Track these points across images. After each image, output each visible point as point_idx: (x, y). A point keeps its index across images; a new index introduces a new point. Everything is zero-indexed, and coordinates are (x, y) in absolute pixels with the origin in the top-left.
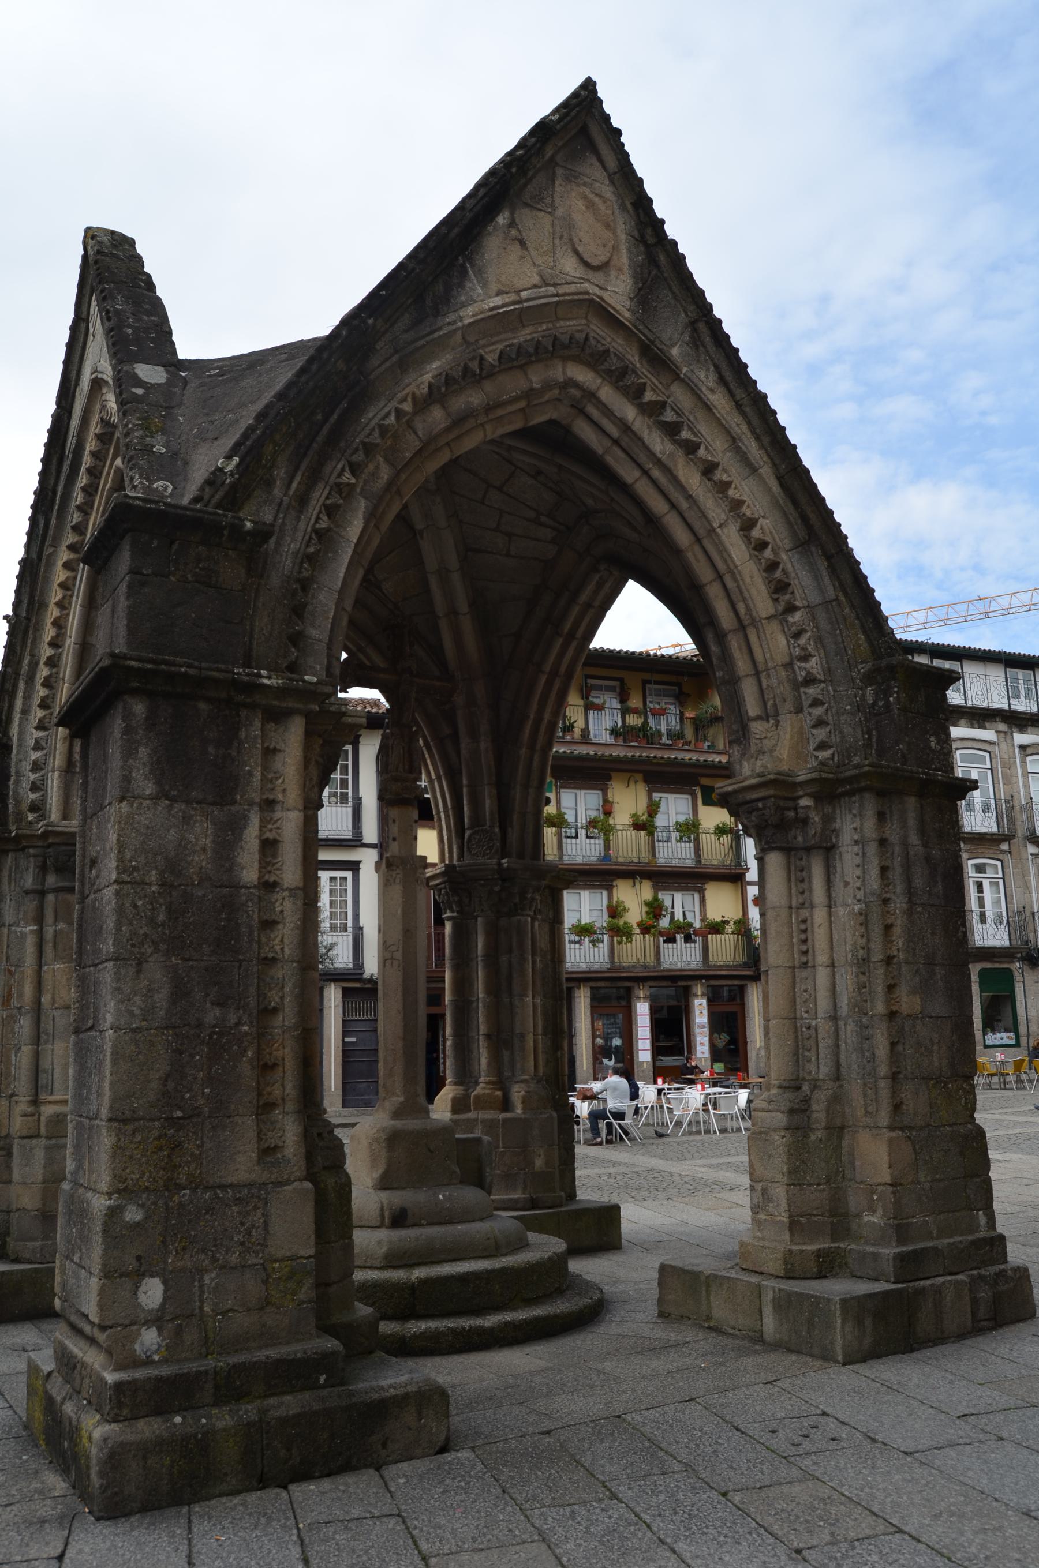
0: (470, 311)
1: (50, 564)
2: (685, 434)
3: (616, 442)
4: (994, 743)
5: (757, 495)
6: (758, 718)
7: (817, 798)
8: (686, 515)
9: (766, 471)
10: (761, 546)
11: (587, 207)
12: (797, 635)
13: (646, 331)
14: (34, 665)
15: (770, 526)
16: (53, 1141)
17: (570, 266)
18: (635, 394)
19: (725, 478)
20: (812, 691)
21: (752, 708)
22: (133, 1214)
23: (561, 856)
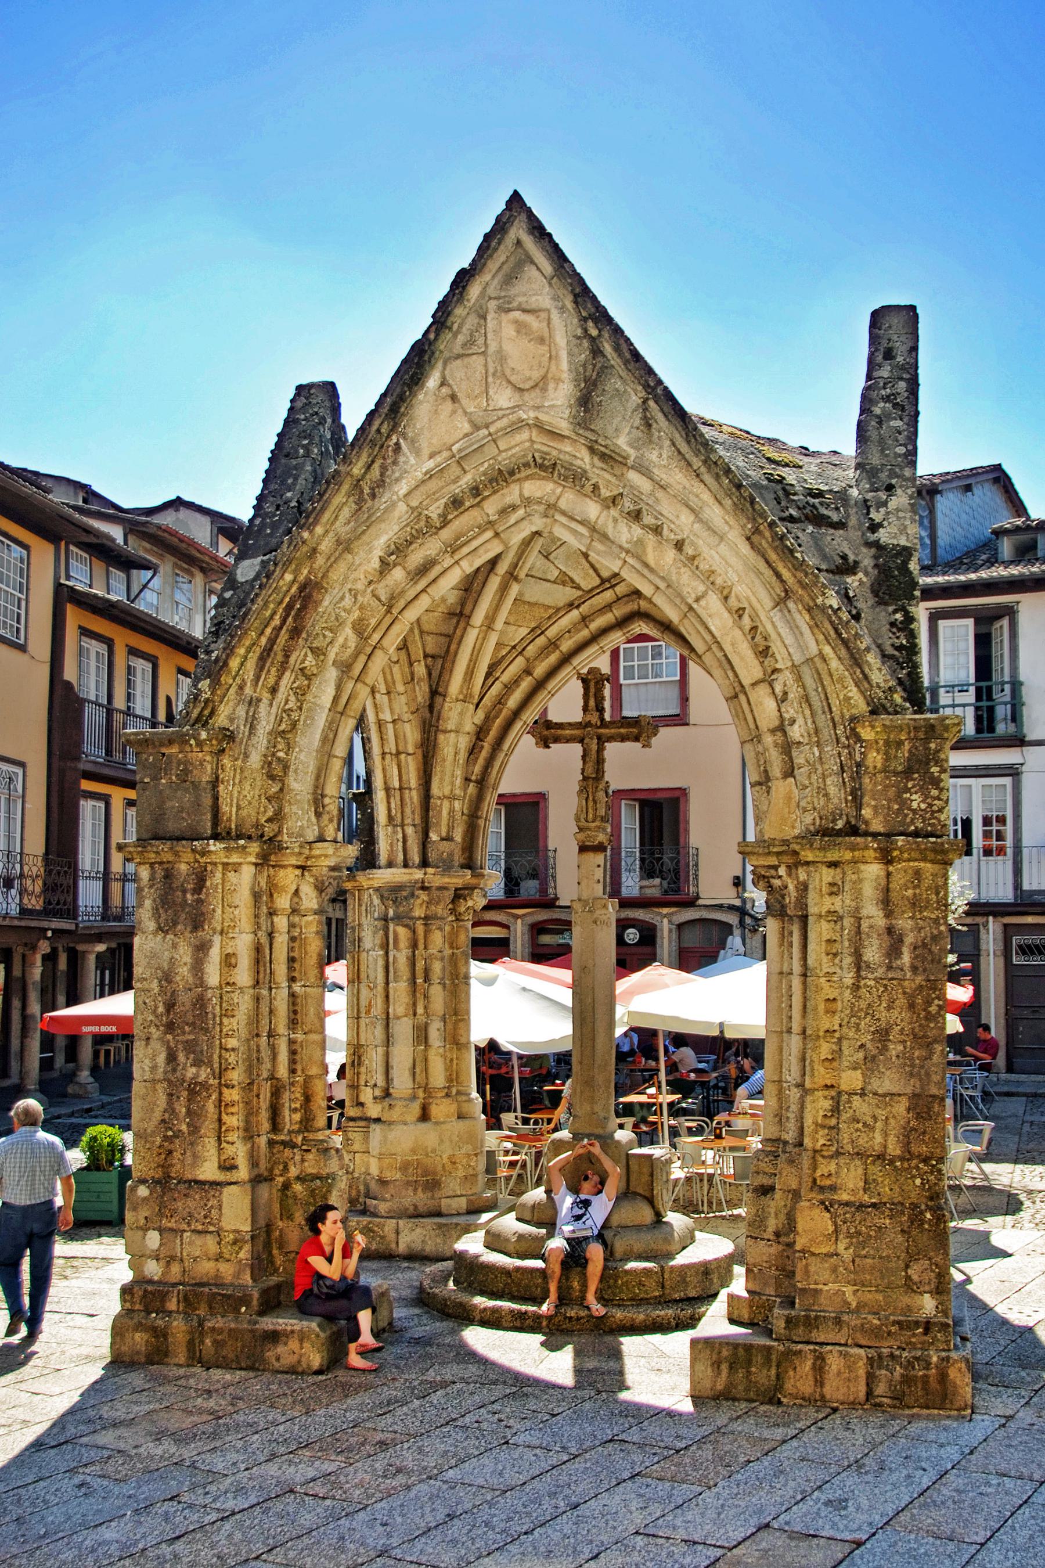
10: (740, 612)
11: (518, 332)
13: (588, 434)
17: (503, 398)
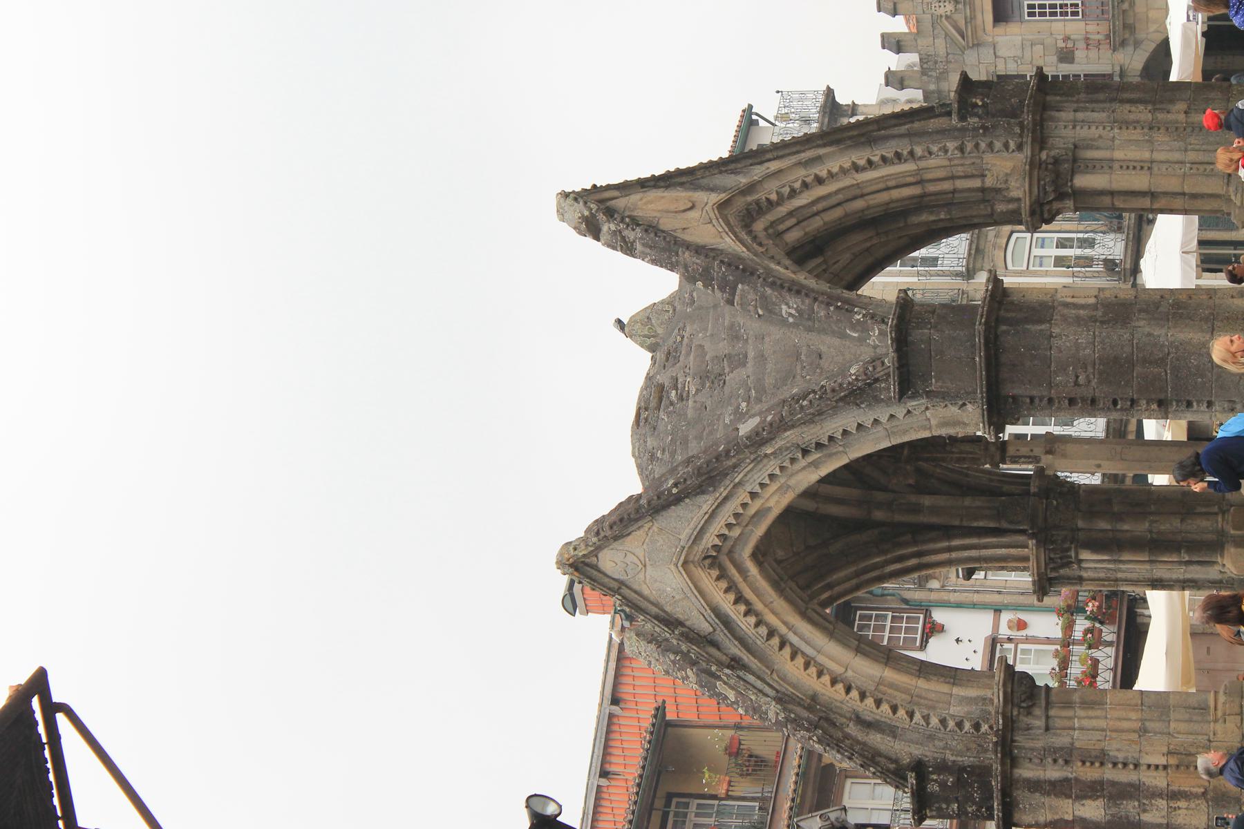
2: (797, 185)
5: (837, 161)
6: (983, 182)
7: (1042, 149)
9: (821, 151)
12: (930, 153)
14: (859, 720)
17: (693, 214)
20: (969, 146)
21: (977, 183)
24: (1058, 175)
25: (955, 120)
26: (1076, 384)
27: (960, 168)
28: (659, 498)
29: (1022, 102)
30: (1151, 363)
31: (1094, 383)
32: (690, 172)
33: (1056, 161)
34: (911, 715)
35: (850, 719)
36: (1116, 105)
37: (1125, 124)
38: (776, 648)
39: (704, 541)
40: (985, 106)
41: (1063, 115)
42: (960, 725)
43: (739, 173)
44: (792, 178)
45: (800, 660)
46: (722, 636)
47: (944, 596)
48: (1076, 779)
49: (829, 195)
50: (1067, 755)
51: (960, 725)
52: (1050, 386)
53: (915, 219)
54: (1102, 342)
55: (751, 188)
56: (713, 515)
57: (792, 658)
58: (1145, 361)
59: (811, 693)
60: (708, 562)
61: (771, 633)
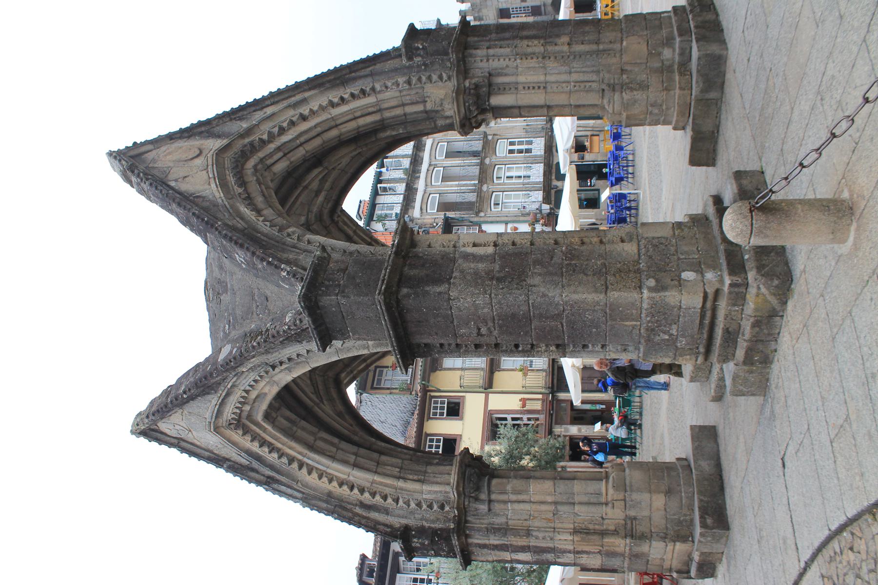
0: (217, 194)
1: (306, 485)
3: (285, 155)
4: (434, 140)
6: (425, 106)
7: (465, 78)
8: (324, 129)
9: (307, 94)
12: (387, 87)
14: (363, 505)
15: (334, 95)
16: (628, 488)
17: (198, 162)
18: (263, 143)
19: (308, 111)
20: (414, 80)
21: (420, 108)
22: (652, 283)
23: (482, 369)
24: (478, 96)
25: (404, 61)
26: (479, 334)
27: (408, 98)
28: (176, 399)
29: (449, 43)
30: (547, 318)
31: (496, 333)
32: (208, 122)
33: (477, 86)
34: (397, 501)
35: (356, 505)
36: (517, 42)
37: (525, 56)
38: (297, 468)
39: (225, 414)
40: (424, 48)
41: (479, 52)
42: (430, 506)
43: (244, 119)
44: (283, 119)
45: (315, 475)
46: (255, 464)
47: (486, 219)
48: (511, 545)
49: (310, 130)
50: (504, 530)
51: (430, 506)
52: (455, 335)
53: (383, 135)
54: (499, 303)
55: (249, 132)
56: (222, 404)
57: (310, 473)
58: (541, 316)
59: (326, 491)
60: (232, 426)
61: (291, 460)
